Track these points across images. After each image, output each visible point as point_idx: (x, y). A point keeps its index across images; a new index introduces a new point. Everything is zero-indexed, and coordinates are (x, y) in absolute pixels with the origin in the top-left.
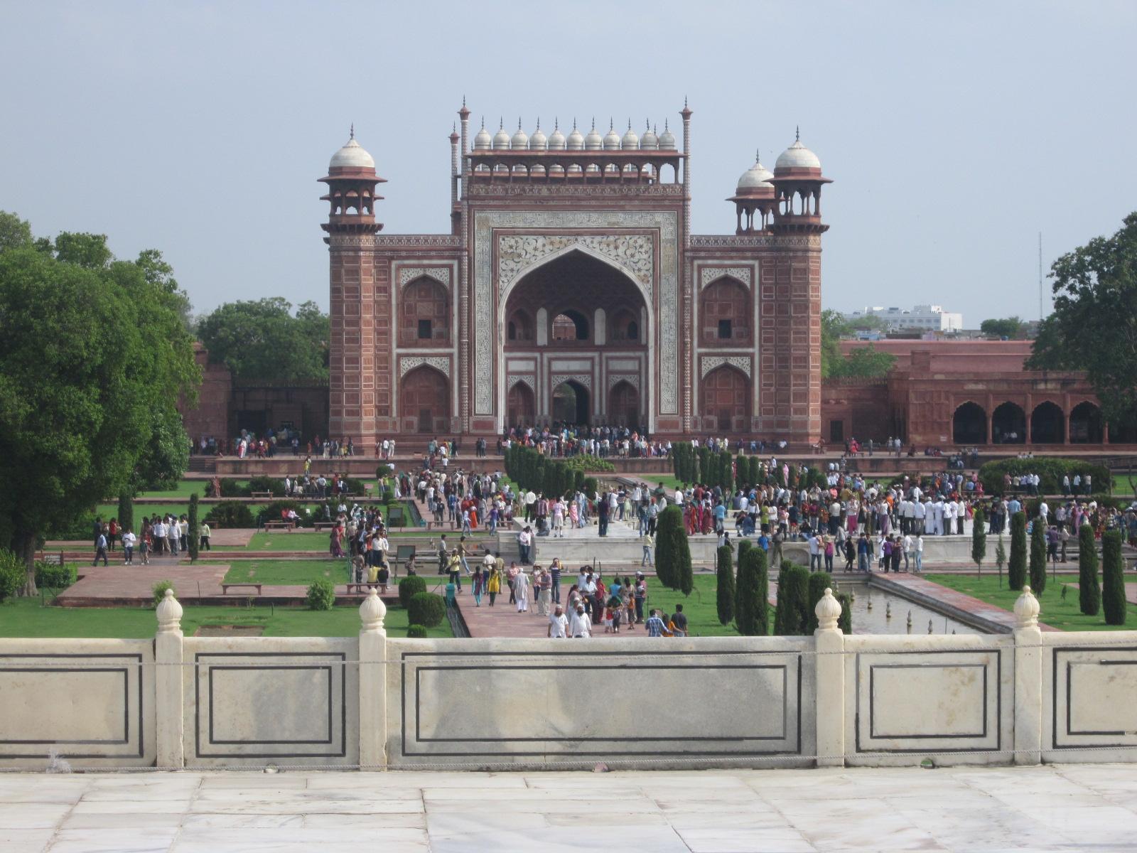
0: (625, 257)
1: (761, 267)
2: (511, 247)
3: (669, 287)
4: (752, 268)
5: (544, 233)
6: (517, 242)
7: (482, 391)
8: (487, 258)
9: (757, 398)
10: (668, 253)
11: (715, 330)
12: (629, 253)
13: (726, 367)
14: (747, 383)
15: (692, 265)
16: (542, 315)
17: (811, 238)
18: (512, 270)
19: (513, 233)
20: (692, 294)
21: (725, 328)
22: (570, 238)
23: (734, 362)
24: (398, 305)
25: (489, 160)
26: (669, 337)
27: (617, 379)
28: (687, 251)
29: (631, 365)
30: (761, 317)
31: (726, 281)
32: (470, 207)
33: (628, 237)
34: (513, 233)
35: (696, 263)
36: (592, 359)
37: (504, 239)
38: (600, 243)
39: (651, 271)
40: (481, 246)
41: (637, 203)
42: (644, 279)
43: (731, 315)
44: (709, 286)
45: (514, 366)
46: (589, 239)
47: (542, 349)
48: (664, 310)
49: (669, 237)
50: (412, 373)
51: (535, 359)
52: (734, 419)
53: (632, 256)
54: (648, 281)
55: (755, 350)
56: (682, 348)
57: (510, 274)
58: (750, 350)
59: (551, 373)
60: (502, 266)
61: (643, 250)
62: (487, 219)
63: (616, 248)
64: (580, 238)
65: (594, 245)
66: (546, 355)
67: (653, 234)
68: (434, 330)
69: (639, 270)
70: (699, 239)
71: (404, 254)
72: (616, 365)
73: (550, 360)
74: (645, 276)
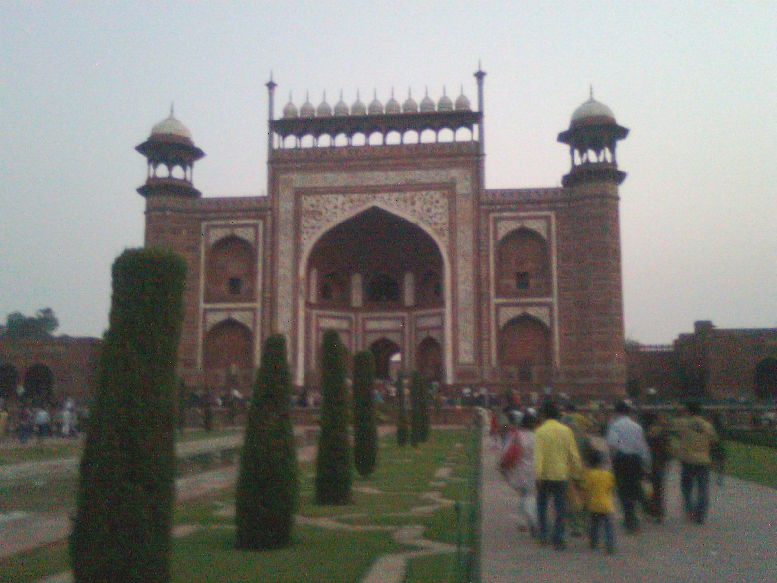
0: (421, 211)
1: (557, 218)
2: (312, 206)
3: (466, 242)
4: (548, 218)
6: (318, 201)
8: (290, 217)
9: (557, 348)
10: (465, 207)
11: (513, 282)
12: (425, 207)
14: (547, 333)
15: (488, 218)
16: (357, 280)
17: (610, 185)
18: (313, 228)
19: (314, 191)
20: (488, 246)
21: (522, 279)
22: (370, 196)
23: (532, 312)
24: (206, 263)
26: (465, 288)
27: (424, 335)
28: (483, 204)
29: (433, 322)
30: (558, 267)
32: (274, 169)
33: (424, 193)
34: (314, 191)
35: (492, 216)
36: (402, 319)
37: (305, 199)
38: (397, 200)
39: (447, 225)
40: (285, 206)
41: (431, 160)
42: (440, 232)
43: (529, 266)
44: (508, 238)
46: (386, 196)
47: (356, 310)
48: (461, 263)
49: (464, 192)
51: (348, 319)
52: (535, 370)
53: (429, 210)
54: (444, 234)
55: (554, 300)
56: (480, 297)
57: (311, 231)
58: (548, 300)
59: (366, 332)
60: (304, 223)
61: (438, 205)
62: (291, 181)
63: (413, 203)
64: (379, 196)
65: (393, 201)
66: (361, 315)
67: (448, 188)
68: (244, 288)
69: (436, 224)
70: (494, 192)
71: (212, 215)
73: (364, 320)
74: (441, 229)
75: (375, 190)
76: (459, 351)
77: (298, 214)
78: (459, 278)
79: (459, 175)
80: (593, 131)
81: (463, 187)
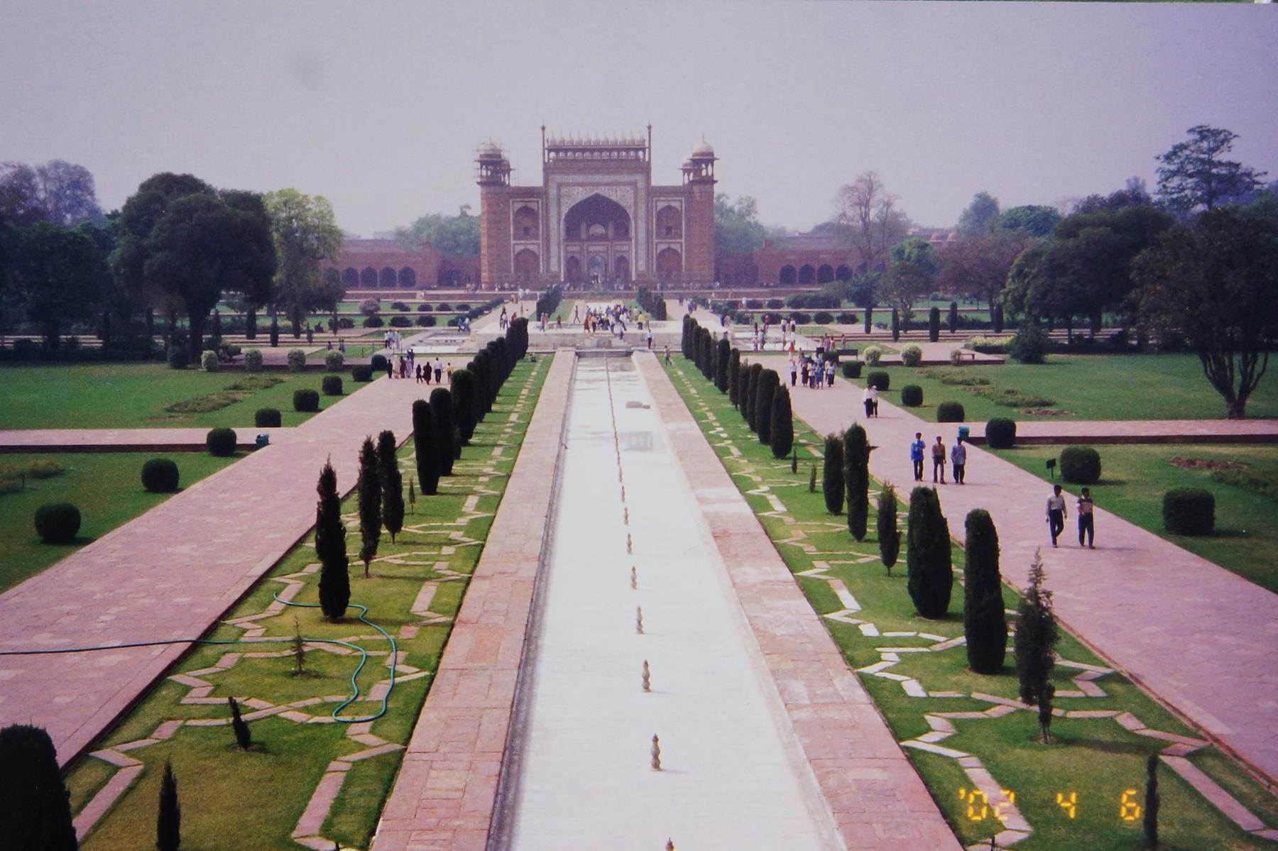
3: (642, 213)
5: (582, 185)
7: (554, 260)
10: (642, 194)
13: (669, 249)
14: (680, 256)
16: (583, 227)
19: (568, 185)
21: (669, 229)
23: (673, 246)
25: (557, 151)
26: (642, 235)
27: (618, 255)
29: (626, 248)
31: (669, 207)
34: (568, 185)
40: (553, 192)
45: (569, 249)
50: (519, 253)
67: (633, 184)
72: (618, 248)
75: (598, 184)
76: (639, 264)
77: (559, 197)
78: (639, 228)
79: (639, 178)
80: (704, 159)
81: (641, 185)
